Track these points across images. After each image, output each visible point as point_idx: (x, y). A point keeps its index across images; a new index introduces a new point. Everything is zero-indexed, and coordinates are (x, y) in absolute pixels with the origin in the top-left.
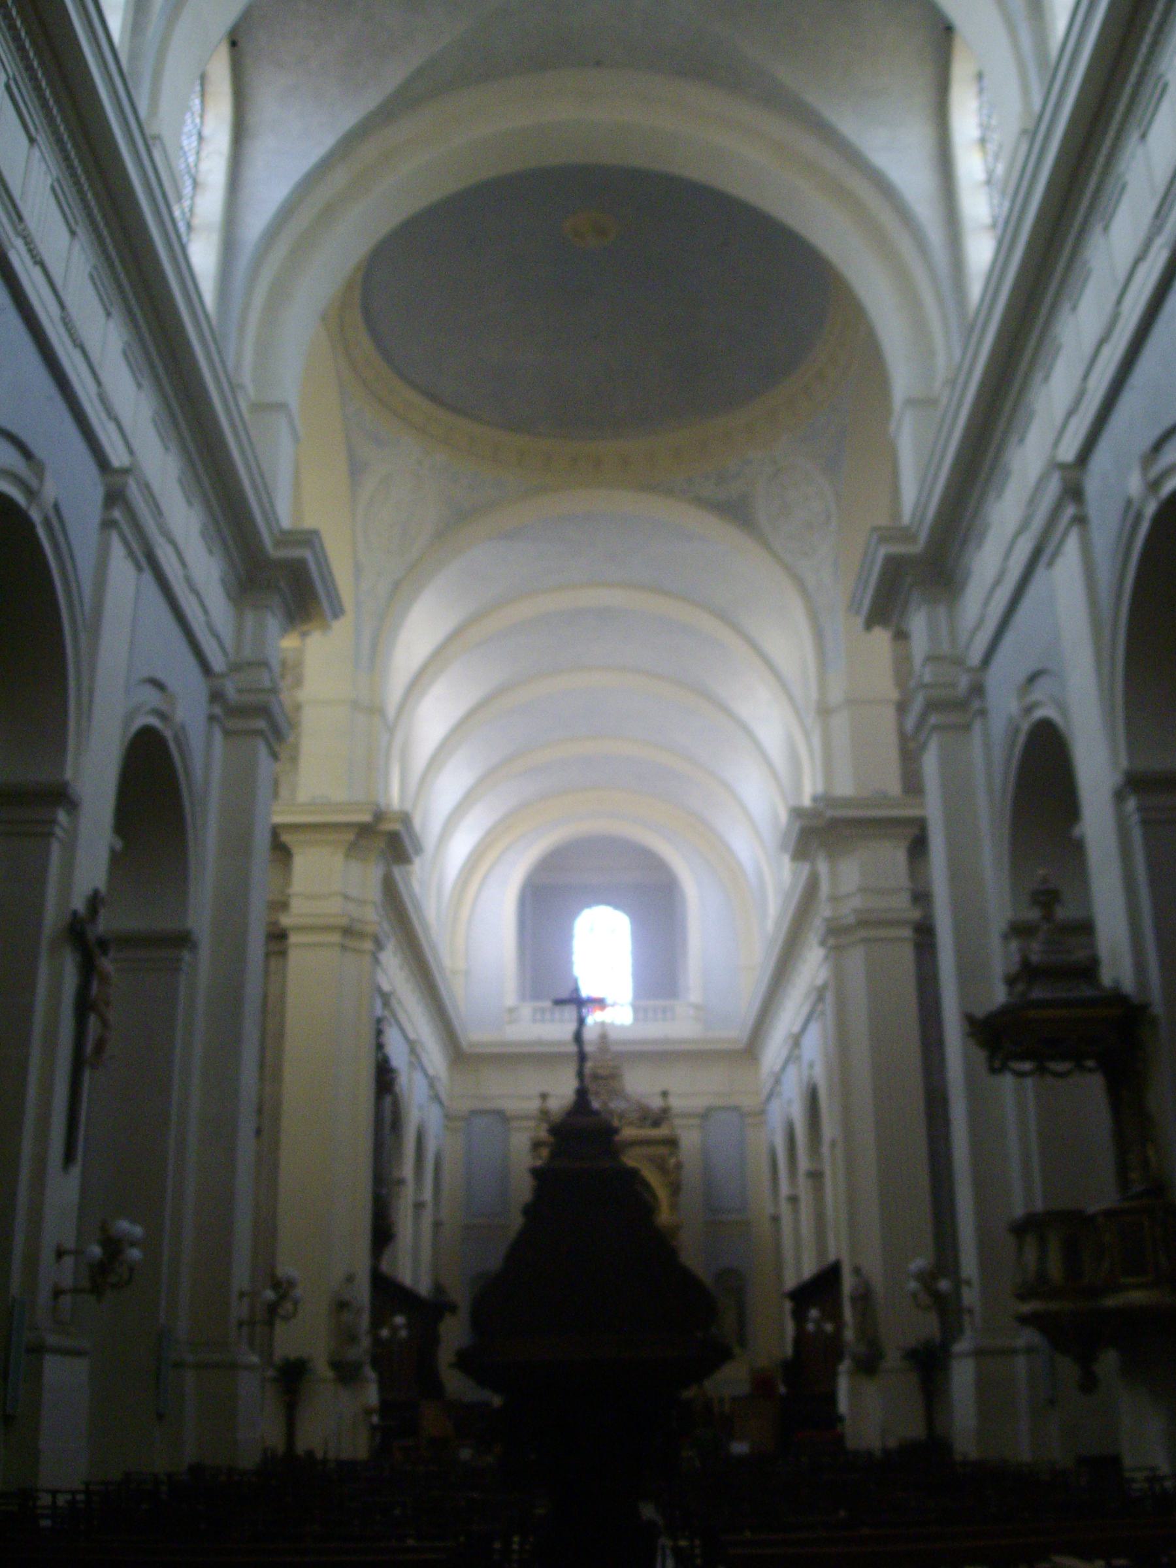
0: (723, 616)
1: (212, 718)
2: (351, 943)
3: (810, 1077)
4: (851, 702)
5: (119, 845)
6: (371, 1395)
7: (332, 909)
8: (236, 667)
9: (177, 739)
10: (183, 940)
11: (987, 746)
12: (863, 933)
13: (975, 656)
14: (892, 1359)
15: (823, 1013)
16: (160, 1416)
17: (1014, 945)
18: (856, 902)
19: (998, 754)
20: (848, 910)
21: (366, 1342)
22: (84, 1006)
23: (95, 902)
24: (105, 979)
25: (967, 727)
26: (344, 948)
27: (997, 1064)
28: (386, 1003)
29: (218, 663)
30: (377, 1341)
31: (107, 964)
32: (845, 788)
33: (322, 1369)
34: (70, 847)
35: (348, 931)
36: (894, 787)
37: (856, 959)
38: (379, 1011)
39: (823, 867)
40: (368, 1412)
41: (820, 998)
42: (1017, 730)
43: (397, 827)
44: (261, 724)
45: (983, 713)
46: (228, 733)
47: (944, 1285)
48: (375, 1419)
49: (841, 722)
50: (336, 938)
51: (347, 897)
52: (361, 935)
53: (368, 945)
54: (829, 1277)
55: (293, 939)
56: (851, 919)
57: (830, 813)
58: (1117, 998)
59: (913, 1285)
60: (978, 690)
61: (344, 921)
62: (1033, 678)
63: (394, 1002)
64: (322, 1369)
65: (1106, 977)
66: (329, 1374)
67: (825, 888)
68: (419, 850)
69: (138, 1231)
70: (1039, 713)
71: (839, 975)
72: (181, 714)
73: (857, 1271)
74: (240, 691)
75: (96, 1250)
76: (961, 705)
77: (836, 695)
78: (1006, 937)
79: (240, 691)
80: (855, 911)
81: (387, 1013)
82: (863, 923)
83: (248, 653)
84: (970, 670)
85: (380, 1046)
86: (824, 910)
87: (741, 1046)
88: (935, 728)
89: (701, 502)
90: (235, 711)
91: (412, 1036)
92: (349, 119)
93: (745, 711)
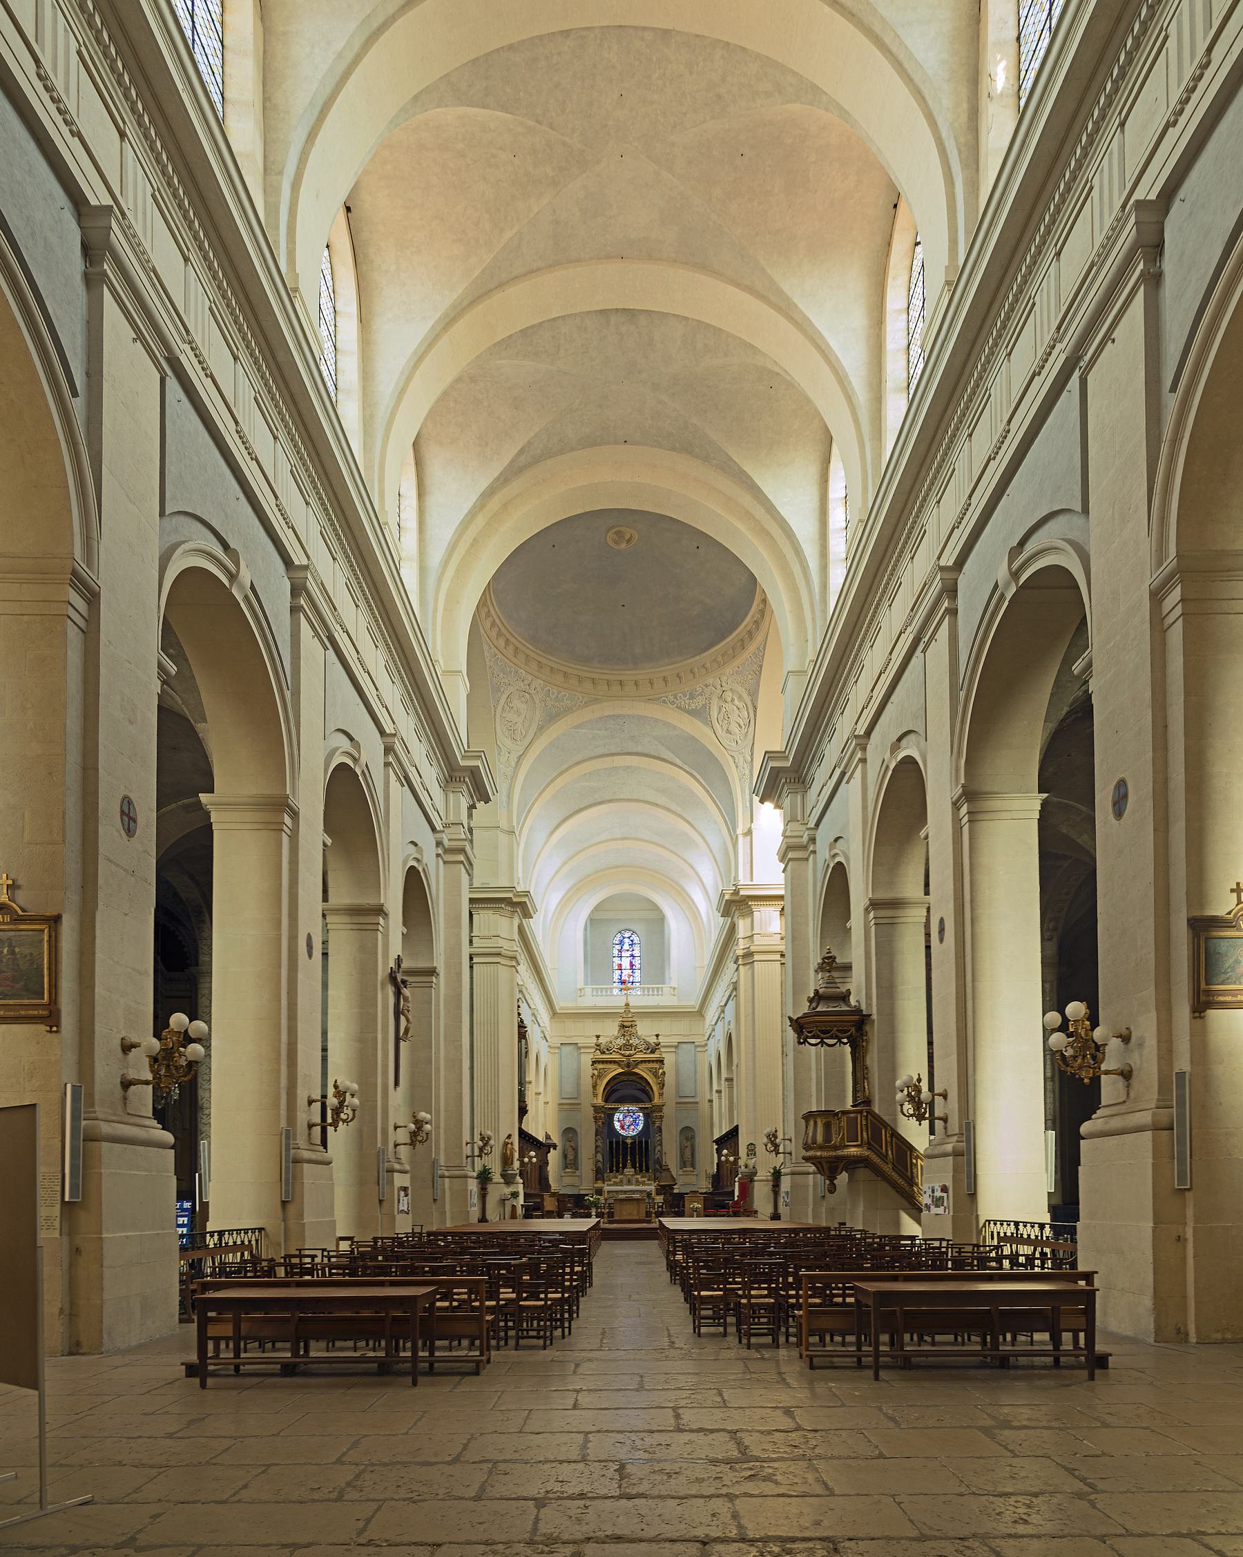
1: (438, 855)
5: (405, 931)
8: (446, 826)
11: (815, 871)
13: (812, 824)
22: (398, 1013)
23: (399, 960)
25: (807, 859)
29: (439, 827)
31: (406, 992)
34: (386, 936)
42: (828, 865)
44: (462, 858)
45: (814, 852)
46: (445, 862)
54: (734, 1133)
58: (858, 1011)
60: (813, 840)
62: (836, 840)
65: (853, 1001)
68: (536, 911)
70: (837, 860)
74: (449, 840)
76: (805, 847)
79: (449, 840)
83: (452, 819)
88: (790, 859)
90: (447, 851)
92: (484, 483)
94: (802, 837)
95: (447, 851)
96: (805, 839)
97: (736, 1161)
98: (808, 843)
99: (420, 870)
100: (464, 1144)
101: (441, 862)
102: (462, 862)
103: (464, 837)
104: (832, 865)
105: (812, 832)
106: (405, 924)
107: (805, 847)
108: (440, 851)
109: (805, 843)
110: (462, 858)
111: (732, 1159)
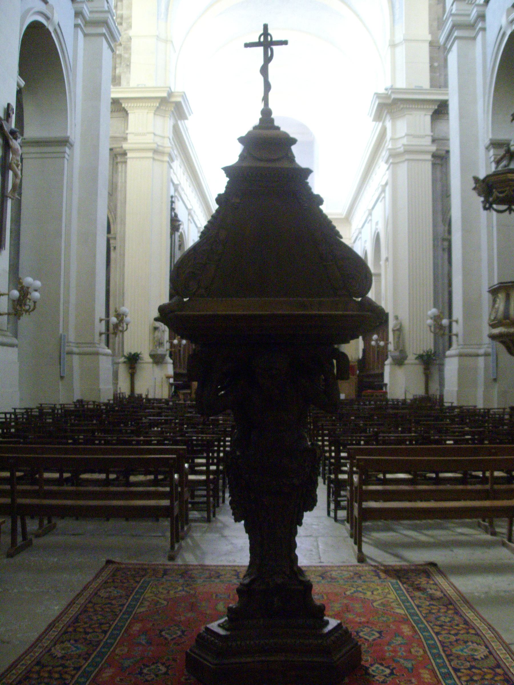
1: (76, 26)
2: (156, 157)
3: (377, 229)
4: (405, 40)
5: (23, 83)
6: (170, 370)
7: (149, 140)
9: (55, 30)
10: (65, 142)
12: (407, 157)
14: (411, 358)
15: (384, 197)
16: (62, 378)
17: (492, 152)
18: (405, 141)
19: (490, 50)
20: (400, 145)
21: (167, 346)
24: (15, 152)
25: (474, 38)
26: (154, 159)
27: (487, 206)
28: (176, 190)
30: (172, 345)
32: (401, 84)
33: (146, 357)
35: (155, 151)
36: (426, 84)
37: (403, 169)
38: (172, 192)
39: (388, 124)
40: (168, 378)
41: (383, 191)
42: (504, 34)
45: (484, 29)
46: (85, 35)
47: (445, 322)
48: (172, 381)
49: (401, 51)
50: (150, 154)
51: (155, 134)
52: (162, 153)
53: (166, 158)
55: (129, 155)
56: (402, 150)
57: (393, 96)
59: (430, 322)
60: (482, 17)
61: (154, 146)
63: (180, 189)
64: (146, 357)
66: (151, 360)
67: (389, 135)
69: (38, 283)
71: (394, 176)
72: (56, 18)
73: (396, 318)
74: (91, 12)
75: (16, 293)
76: (472, 26)
77: (399, 37)
78: (487, 149)
80: (404, 145)
81: (176, 194)
82: (406, 152)
84: (478, 5)
85: (173, 209)
86: (389, 145)
87: (343, 217)
88: (456, 38)
90: (89, 23)
91: (189, 207)
94: (469, 15)
95: (89, 23)
96: (474, 13)
97: (387, 344)
98: (476, 21)
99: (51, 30)
100: (97, 320)
101: (80, 35)
102: (104, 35)
103: (107, 9)
104: (509, 33)
105: (481, 9)
106: (22, 73)
107: (472, 26)
108: (79, 22)
109: (472, 21)
110: (104, 30)
111: (382, 343)
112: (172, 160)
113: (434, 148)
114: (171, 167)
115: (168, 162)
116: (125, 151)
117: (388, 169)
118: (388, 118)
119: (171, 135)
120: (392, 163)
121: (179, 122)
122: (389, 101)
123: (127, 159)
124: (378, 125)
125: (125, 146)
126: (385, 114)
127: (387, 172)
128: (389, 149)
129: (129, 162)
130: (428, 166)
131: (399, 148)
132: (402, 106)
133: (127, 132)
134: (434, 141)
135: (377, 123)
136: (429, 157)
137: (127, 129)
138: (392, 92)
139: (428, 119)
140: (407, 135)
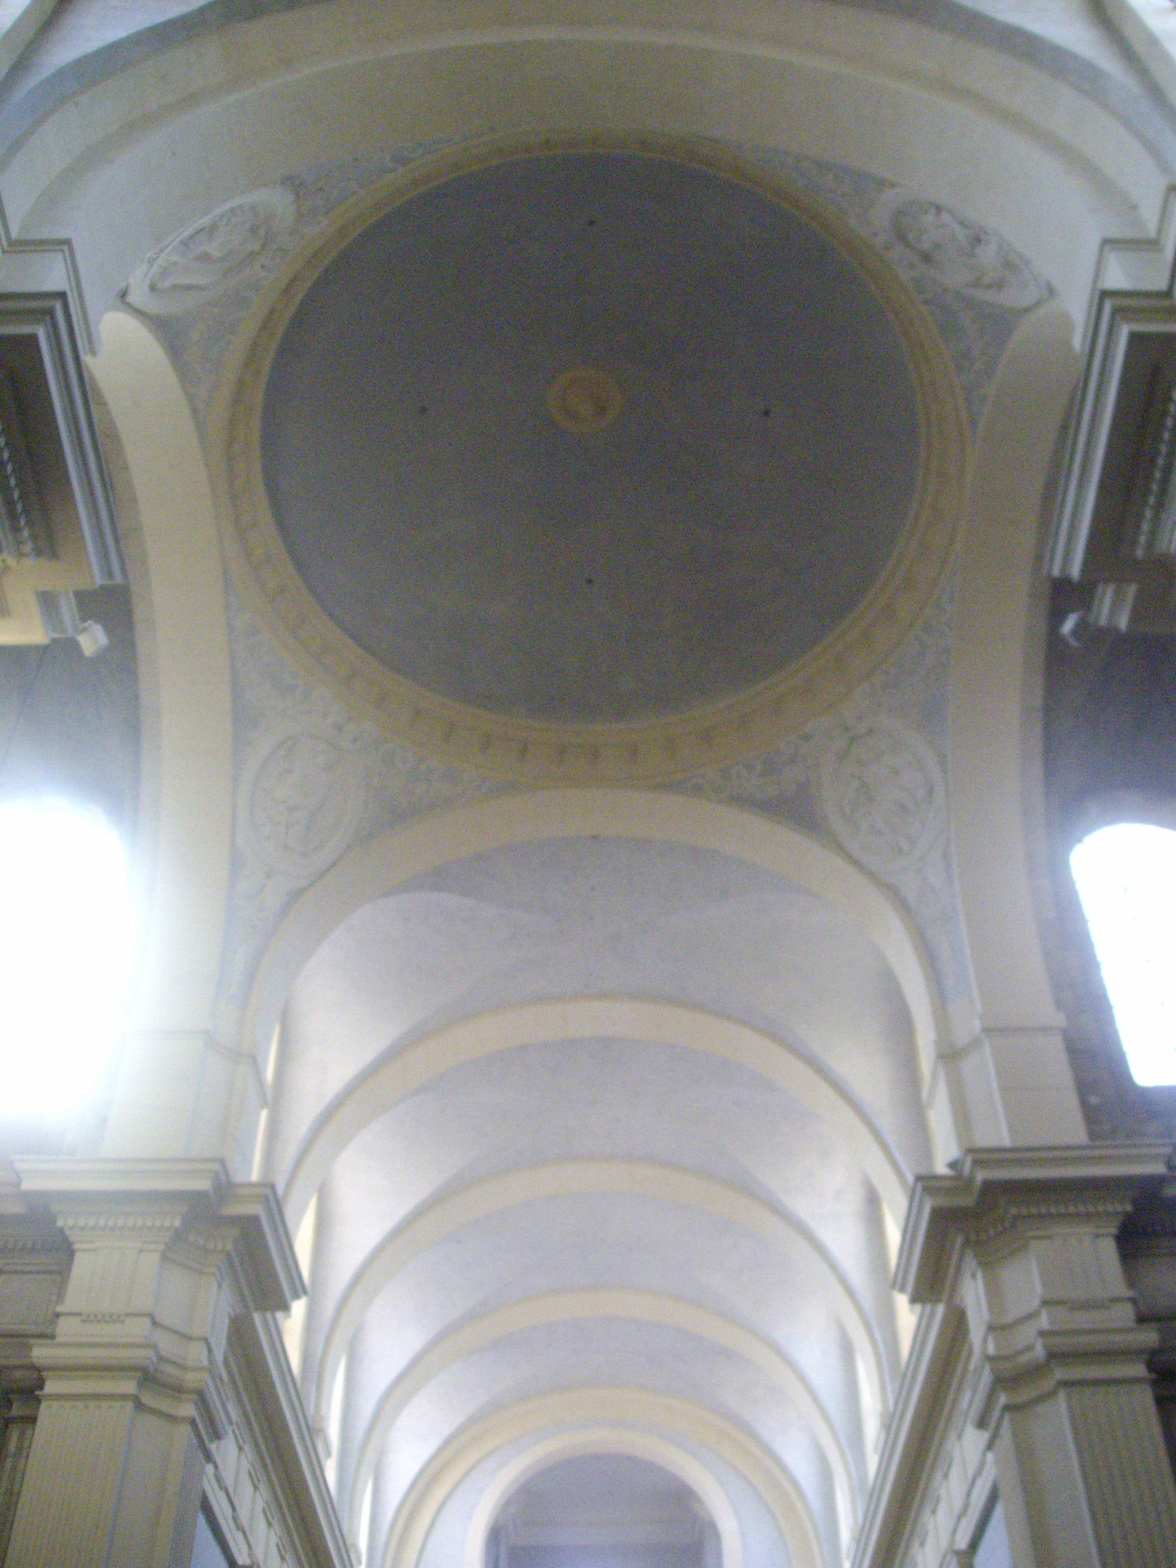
0: (774, 1033)
4: (987, 1030)
12: (1059, 1374)
26: (139, 1406)
35: (147, 1377)
43: (254, 1209)
50: (129, 1386)
51: (155, 1323)
52: (177, 1390)
53: (188, 1409)
55: (50, 1387)
56: (1039, 1351)
57: (980, 1176)
80: (1042, 1333)
82: (1056, 1356)
89: (741, 801)
93: (803, 1208)
112: (217, 1435)
113: (1149, 1337)
114: (208, 1457)
115: (193, 1422)
116: (39, 1370)
117: (990, 1446)
118: (970, 1262)
119: (220, 1345)
120: (1007, 1408)
121: (257, 1317)
122: (967, 1201)
123: (38, 1400)
124: (932, 1316)
125: (41, 1353)
126: (958, 1246)
127: (990, 1457)
128: (990, 1359)
129: (47, 1413)
130: (1144, 1398)
131: (1030, 1348)
132: (1014, 1211)
133: (59, 1309)
134: (1142, 1319)
135: (928, 1307)
136: (1139, 1370)
137: (61, 1298)
138: (977, 1163)
139: (1108, 1249)
140: (1045, 1303)
